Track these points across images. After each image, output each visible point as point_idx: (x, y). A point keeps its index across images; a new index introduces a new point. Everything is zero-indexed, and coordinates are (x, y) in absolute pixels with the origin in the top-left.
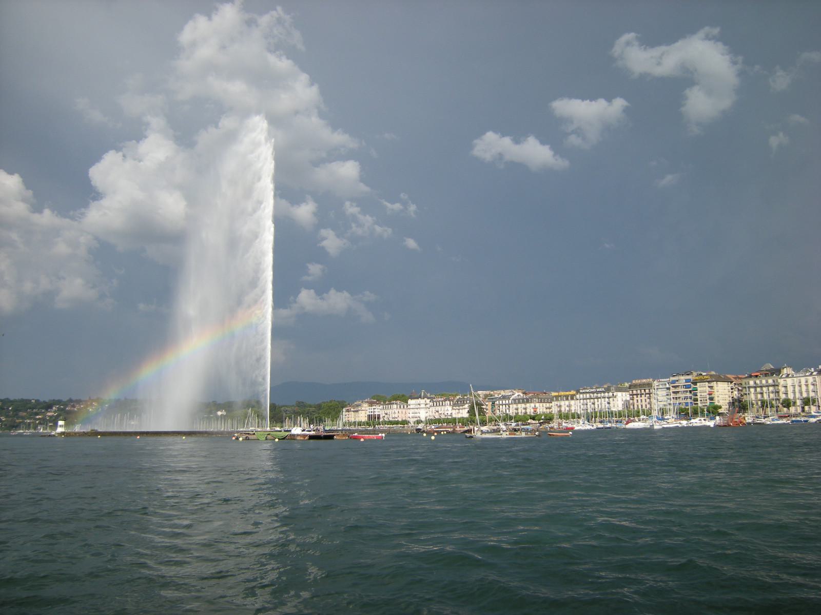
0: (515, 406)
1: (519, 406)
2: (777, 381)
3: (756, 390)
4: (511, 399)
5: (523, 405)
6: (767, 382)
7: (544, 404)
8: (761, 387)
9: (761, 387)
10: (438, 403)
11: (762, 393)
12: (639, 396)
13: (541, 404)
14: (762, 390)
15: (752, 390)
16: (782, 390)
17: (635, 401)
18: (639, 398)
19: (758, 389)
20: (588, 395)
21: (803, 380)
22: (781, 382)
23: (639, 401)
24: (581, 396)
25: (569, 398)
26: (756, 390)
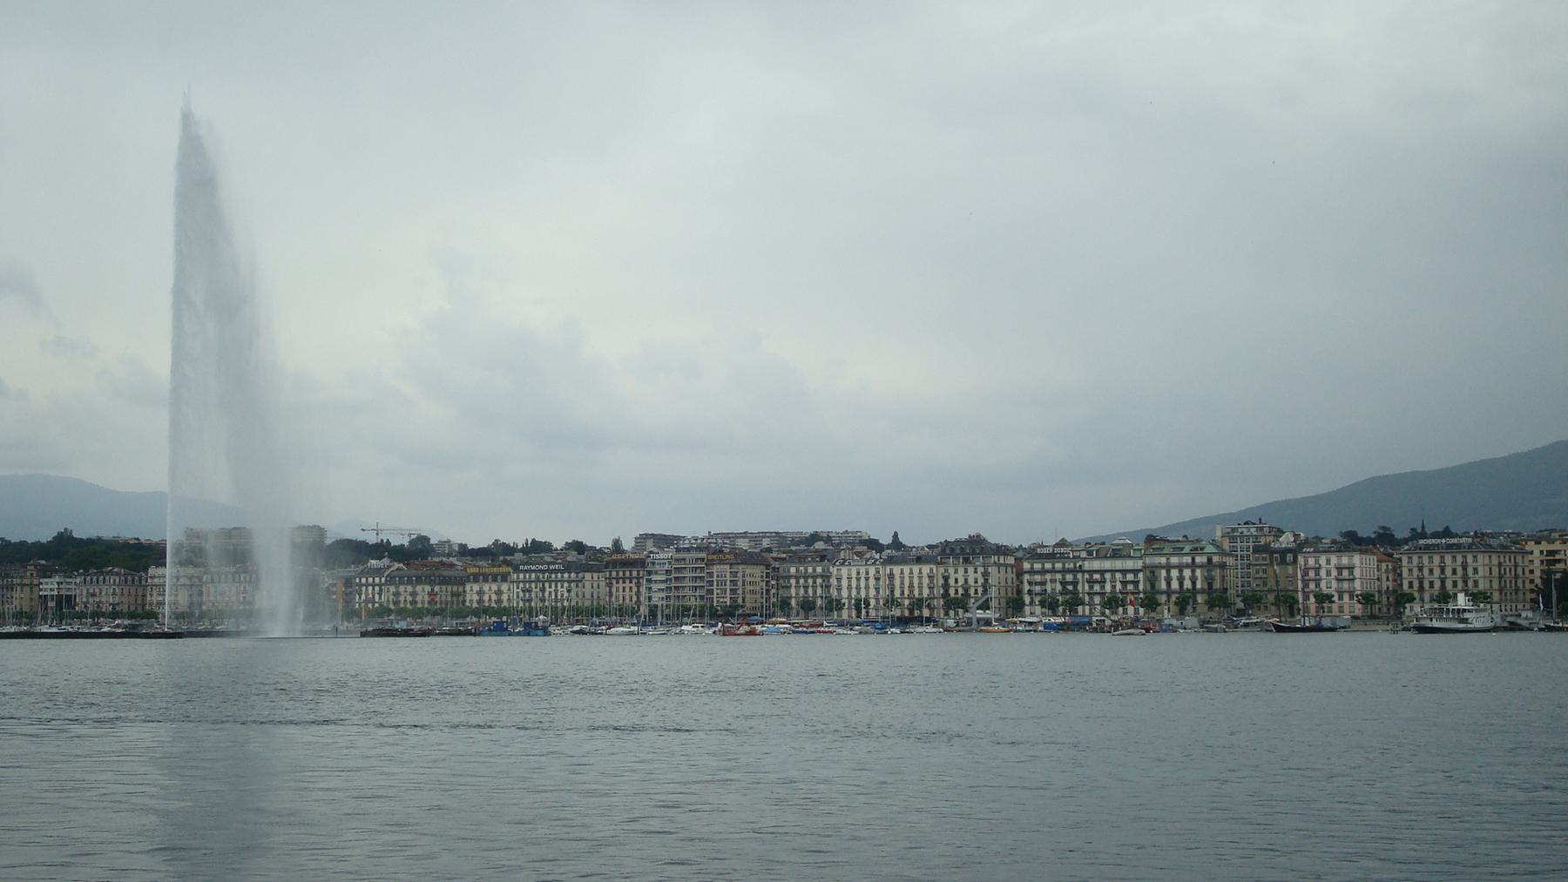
0: (392, 589)
1: (402, 589)
2: (828, 569)
3: (798, 582)
4: (386, 574)
5: (410, 588)
6: (814, 570)
7: (449, 588)
8: (806, 578)
9: (806, 578)
10: (223, 577)
11: (806, 588)
12: (621, 581)
13: (444, 587)
14: (806, 581)
15: (793, 581)
16: (833, 581)
17: (614, 590)
18: (621, 585)
19: (802, 581)
20: (533, 575)
21: (862, 570)
22: (834, 570)
23: (621, 589)
24: (521, 576)
25: (499, 577)
26: (798, 582)
